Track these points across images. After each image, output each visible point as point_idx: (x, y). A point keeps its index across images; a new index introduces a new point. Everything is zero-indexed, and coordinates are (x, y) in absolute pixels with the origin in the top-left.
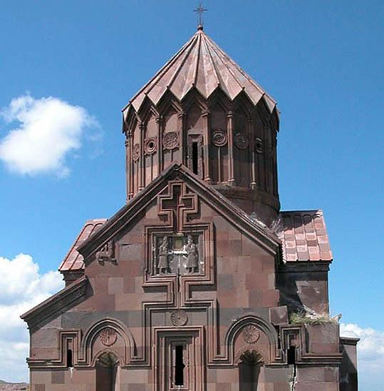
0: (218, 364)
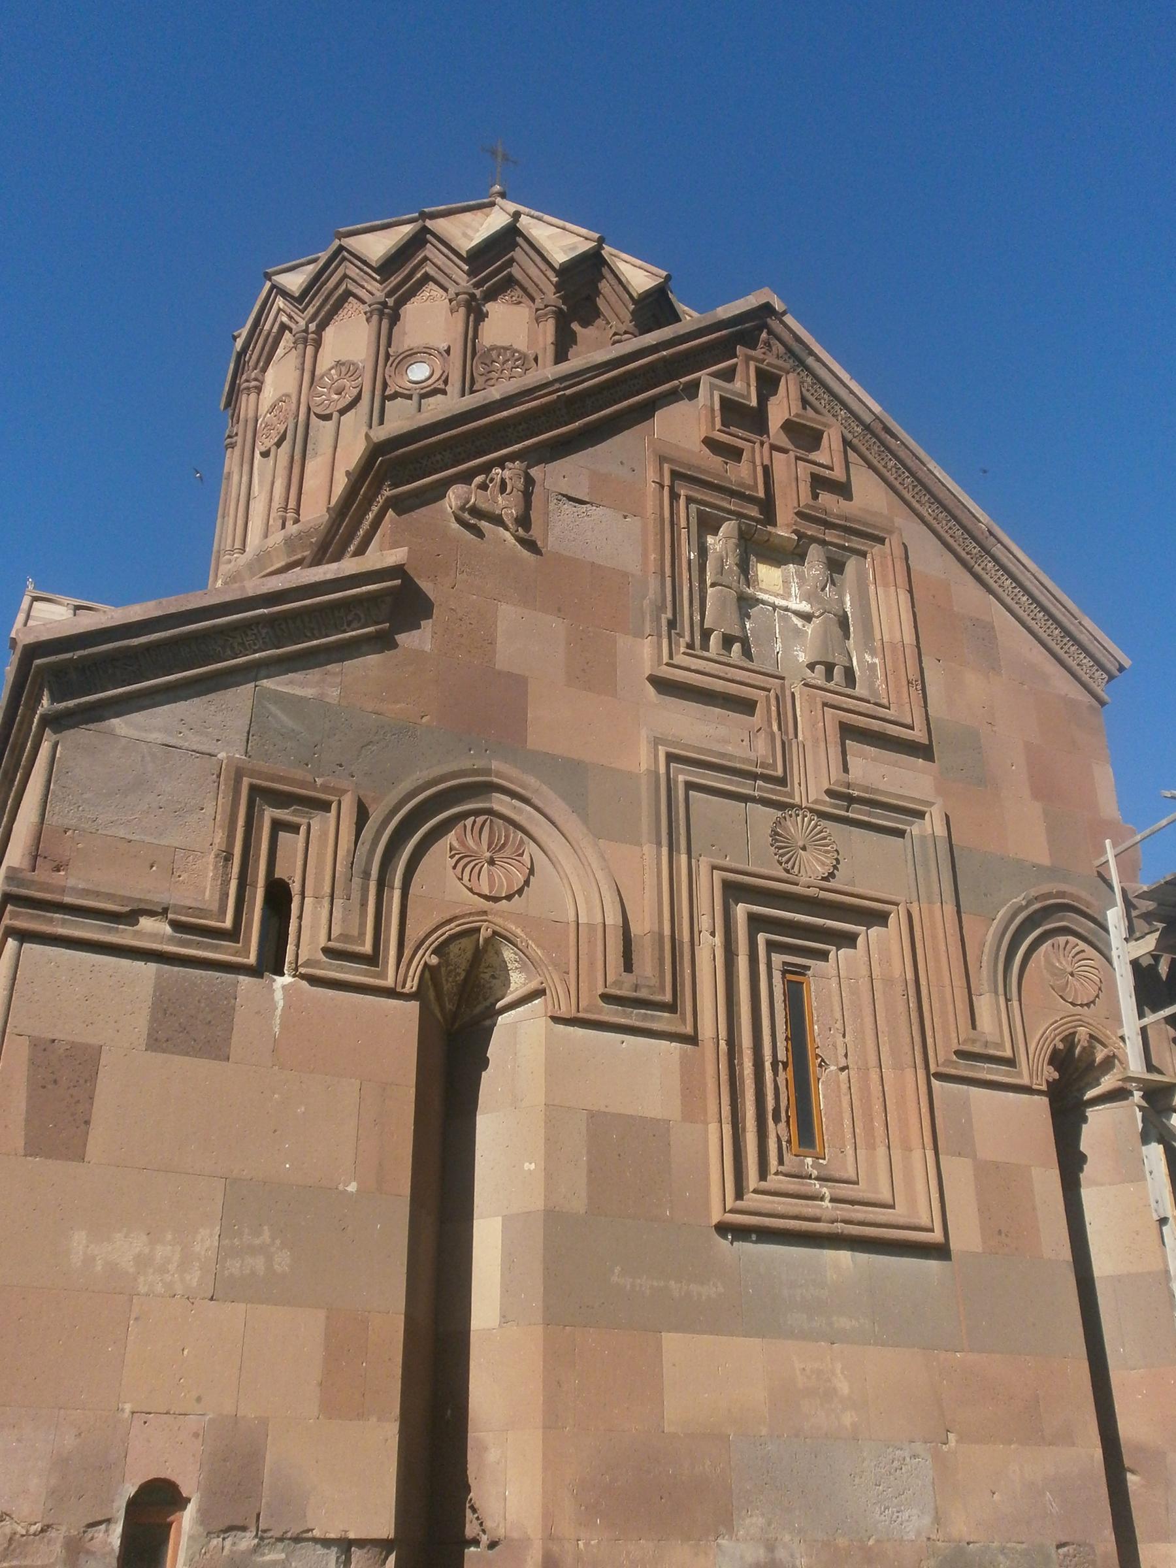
0: (977, 1065)
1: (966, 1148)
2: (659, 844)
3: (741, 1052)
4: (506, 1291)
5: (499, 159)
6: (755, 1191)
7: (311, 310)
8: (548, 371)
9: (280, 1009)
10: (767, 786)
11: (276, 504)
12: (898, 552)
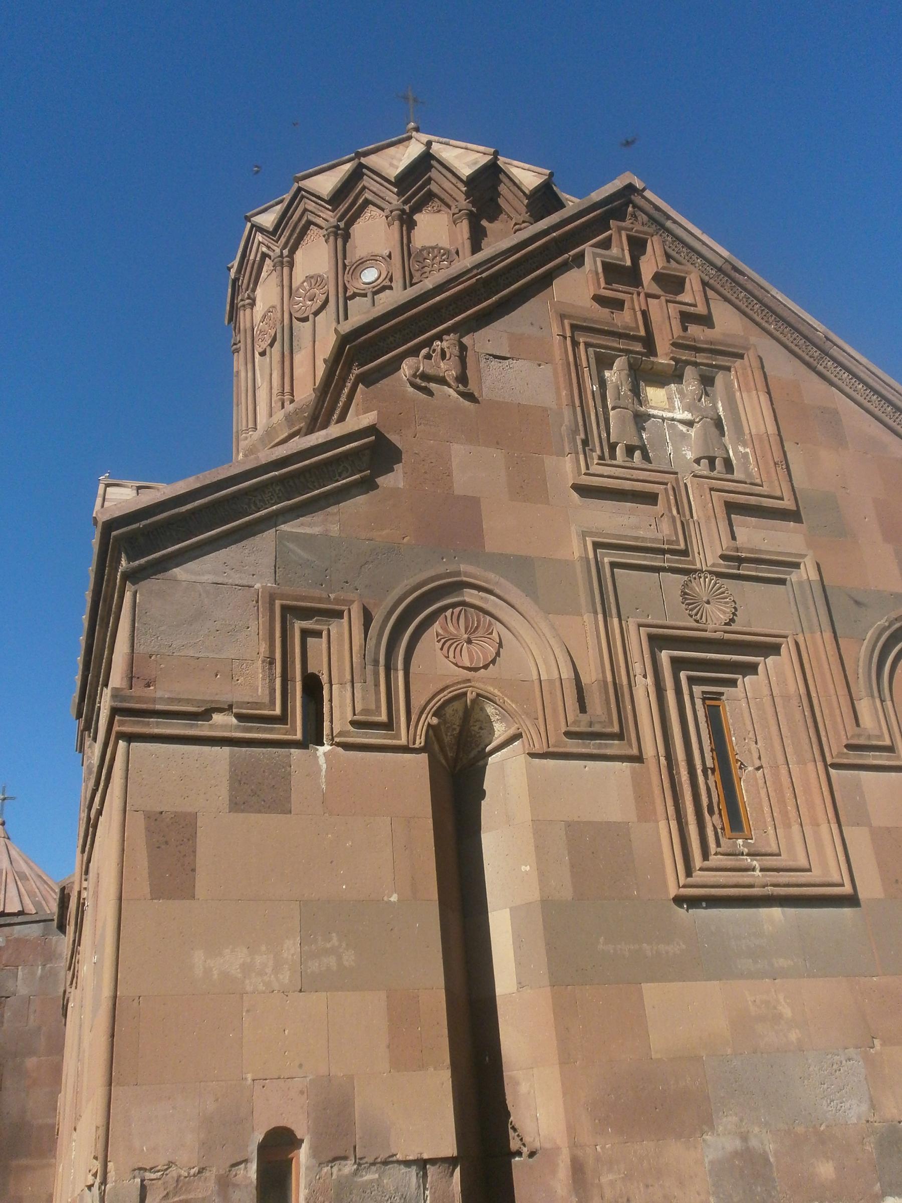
1: (862, 820)
2: (596, 613)
3: (677, 765)
4: (519, 964)
5: (411, 102)
6: (701, 869)
7: (283, 240)
8: (467, 261)
9: (324, 770)
10: (673, 558)
11: (275, 391)
12: (756, 364)
